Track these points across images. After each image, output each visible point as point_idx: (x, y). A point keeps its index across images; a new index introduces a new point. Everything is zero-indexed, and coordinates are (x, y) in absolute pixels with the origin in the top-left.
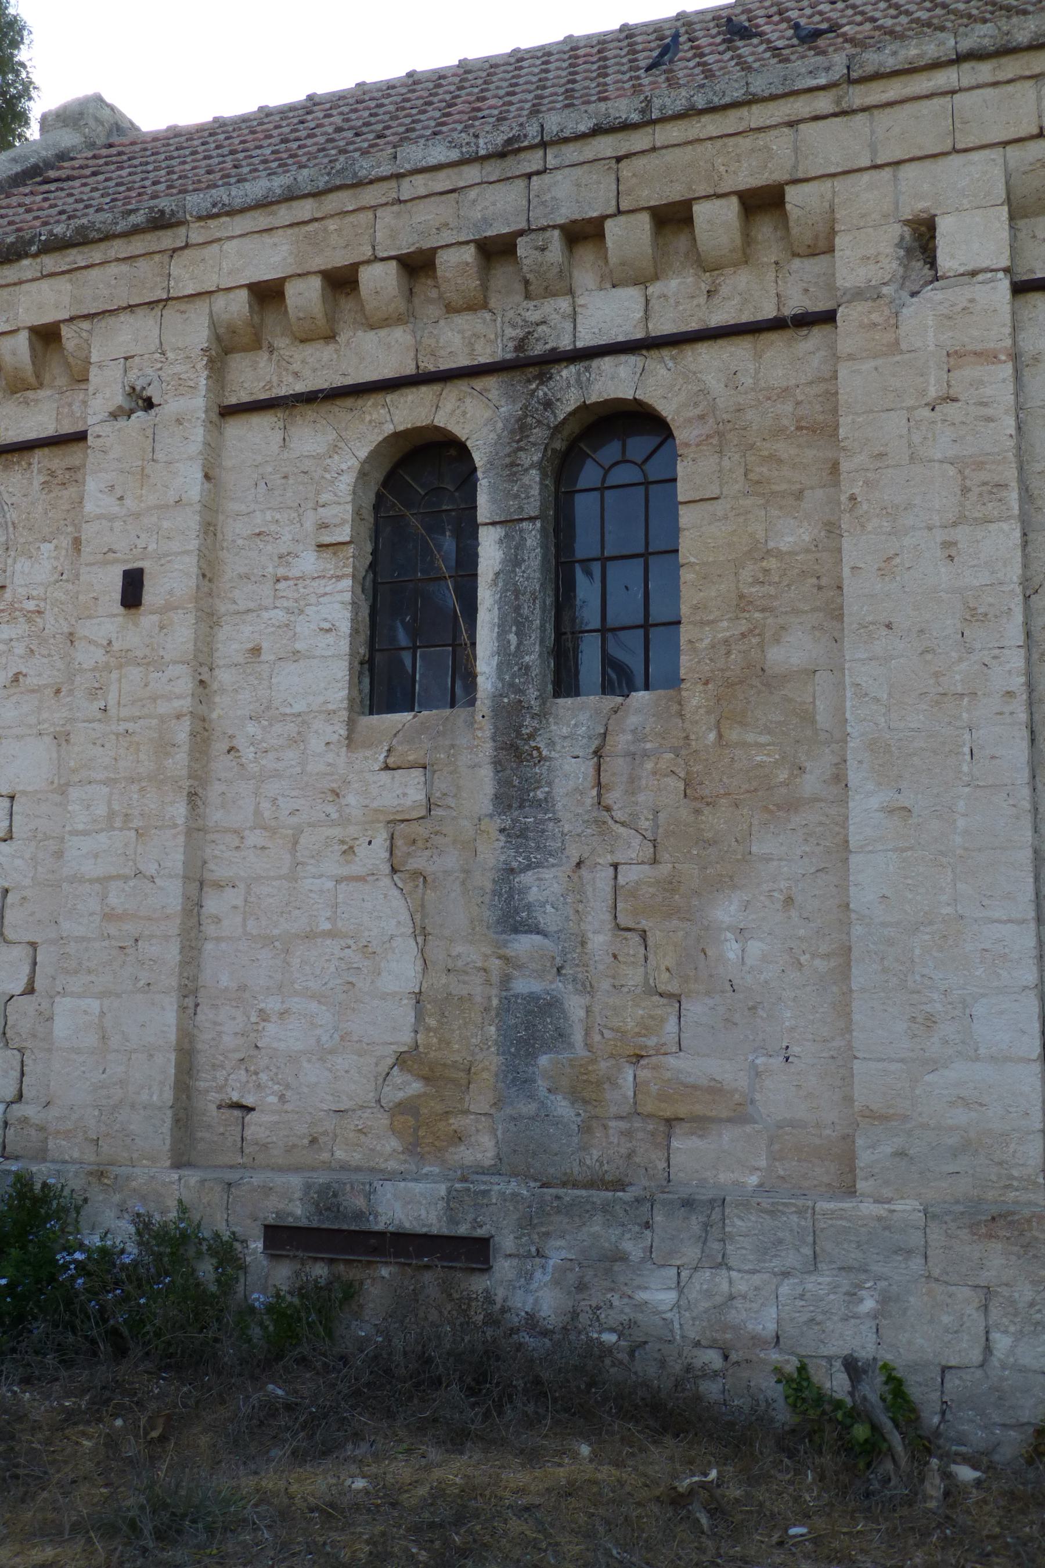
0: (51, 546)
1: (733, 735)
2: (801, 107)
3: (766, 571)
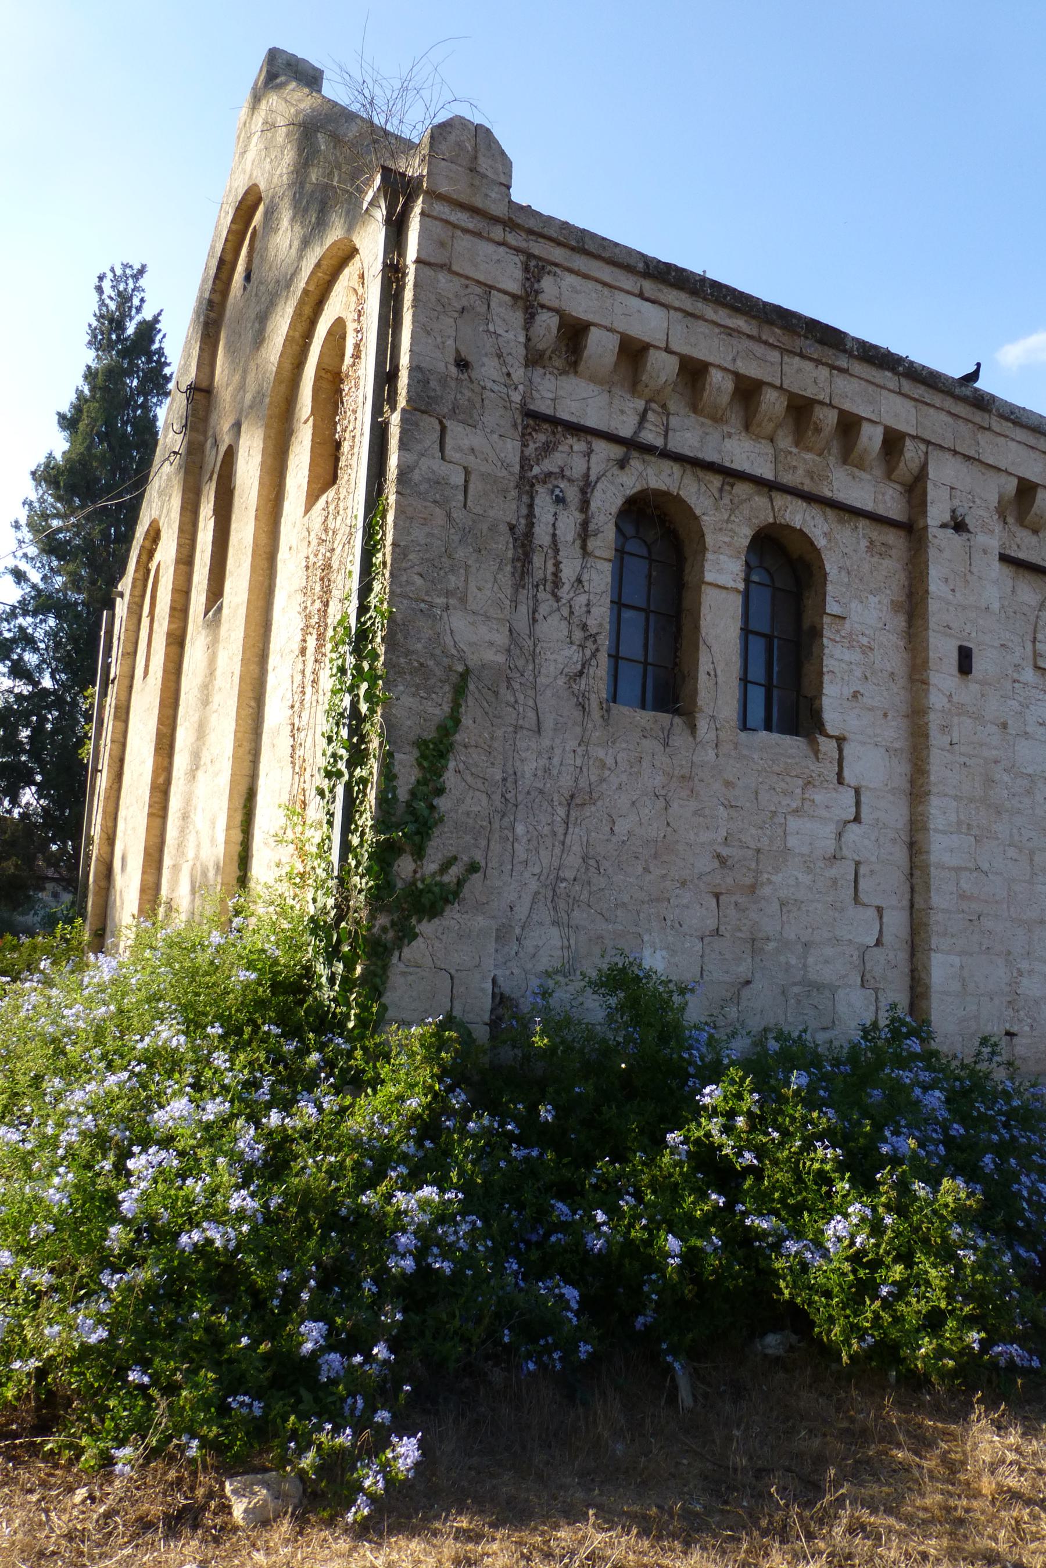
0: (876, 600)
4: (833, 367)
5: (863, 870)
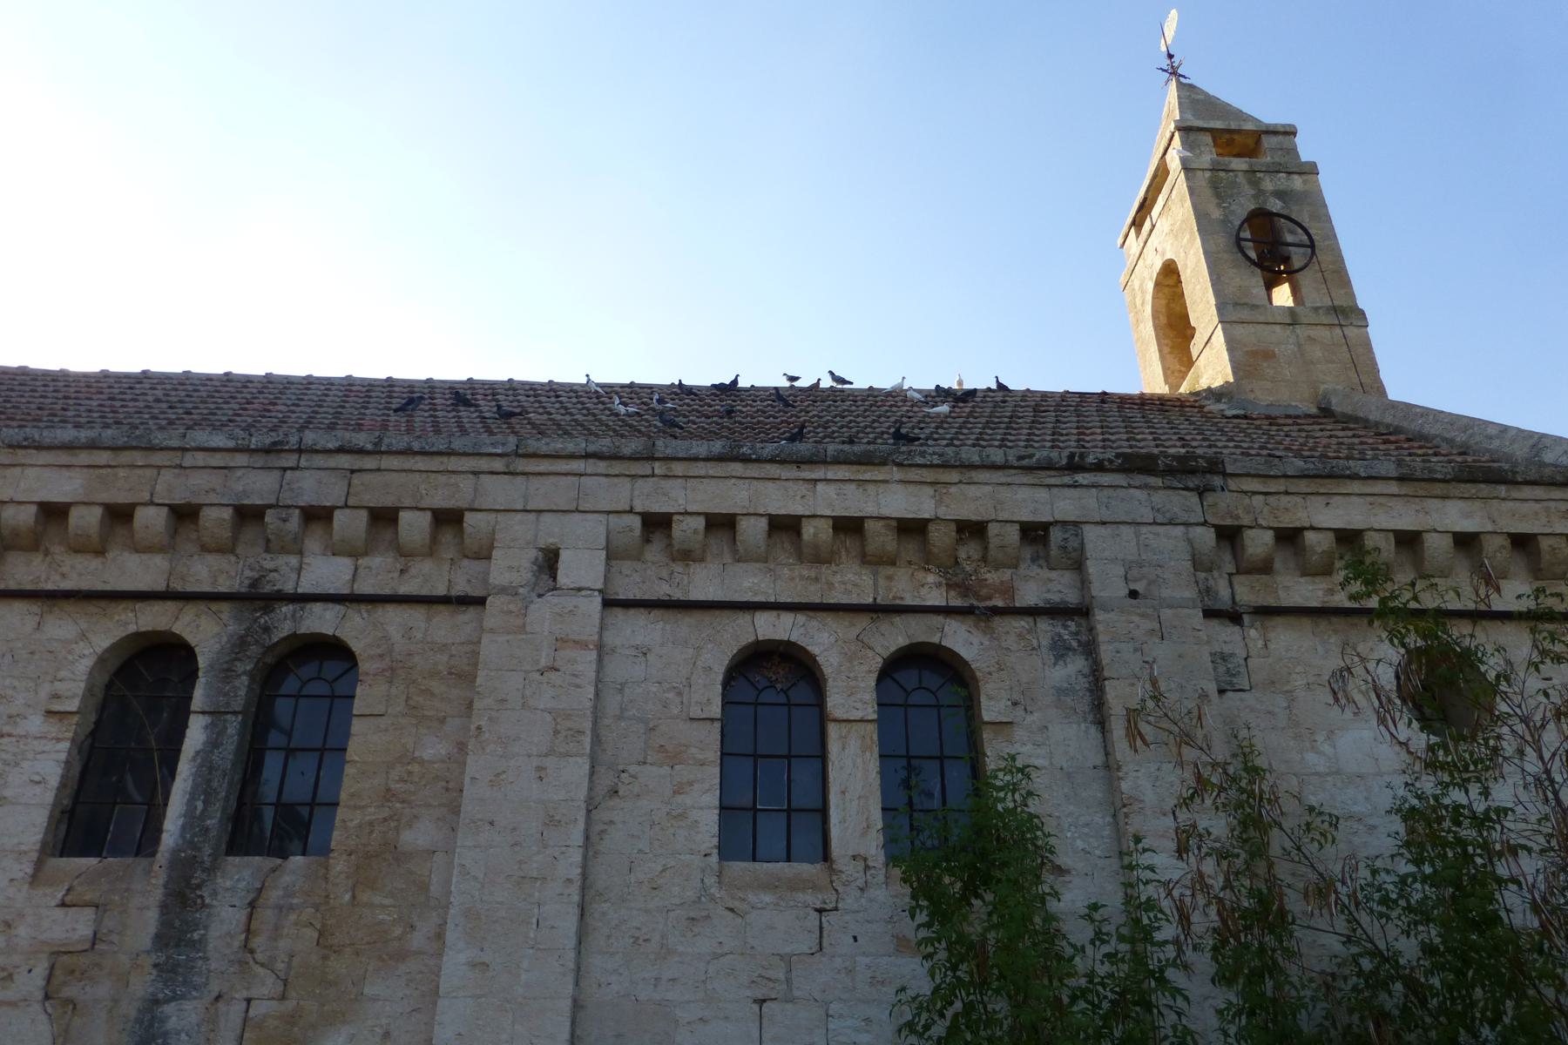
1: (364, 897)
2: (483, 464)
3: (410, 773)
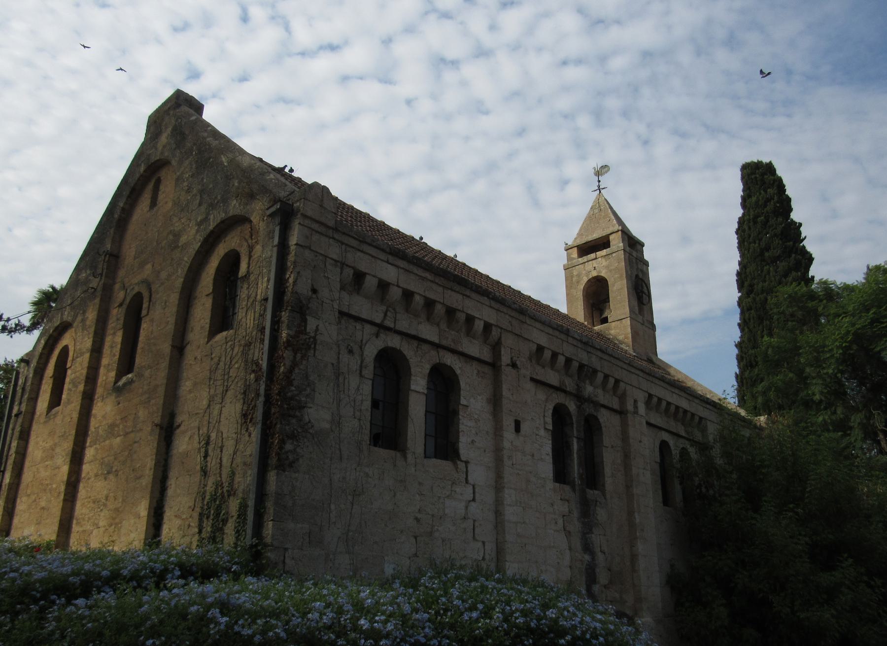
4: (464, 295)
5: (477, 524)
